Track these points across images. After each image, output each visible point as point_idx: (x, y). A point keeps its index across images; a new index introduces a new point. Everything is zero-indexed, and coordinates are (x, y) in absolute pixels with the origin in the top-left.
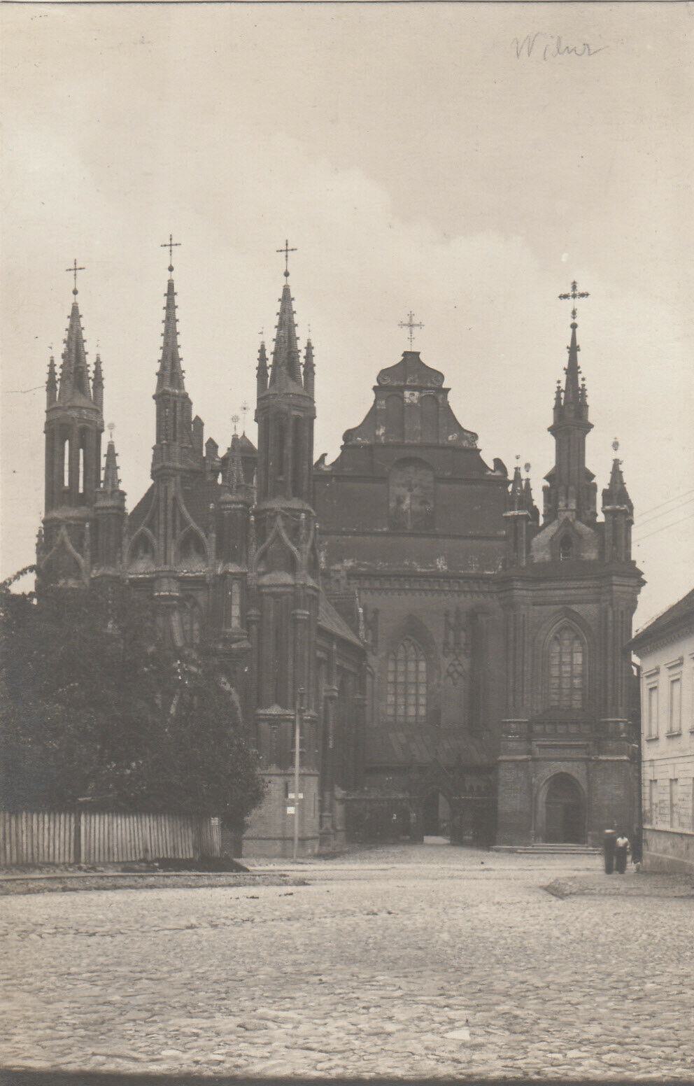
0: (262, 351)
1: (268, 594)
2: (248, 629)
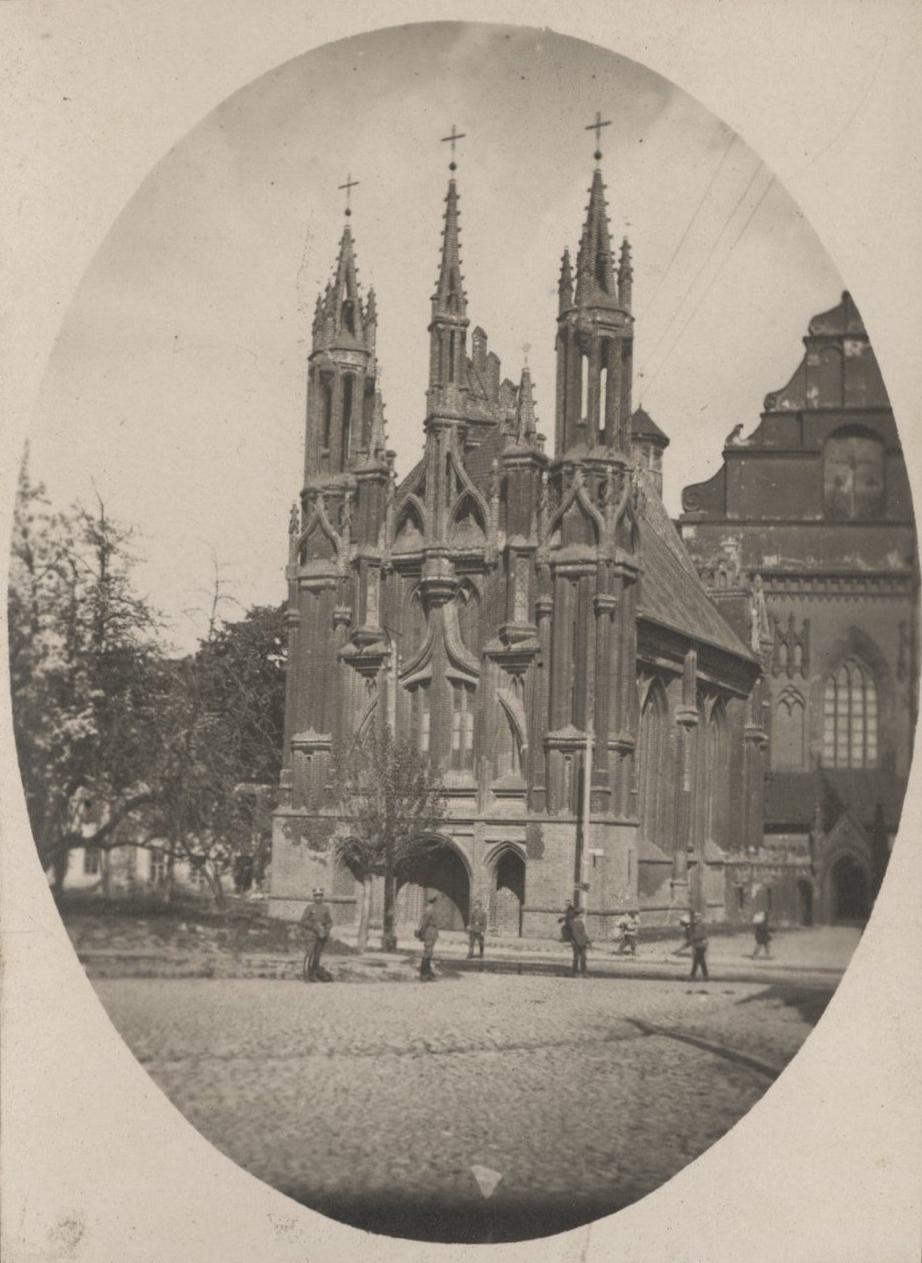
0: (565, 259)
1: (562, 575)
2: (537, 624)
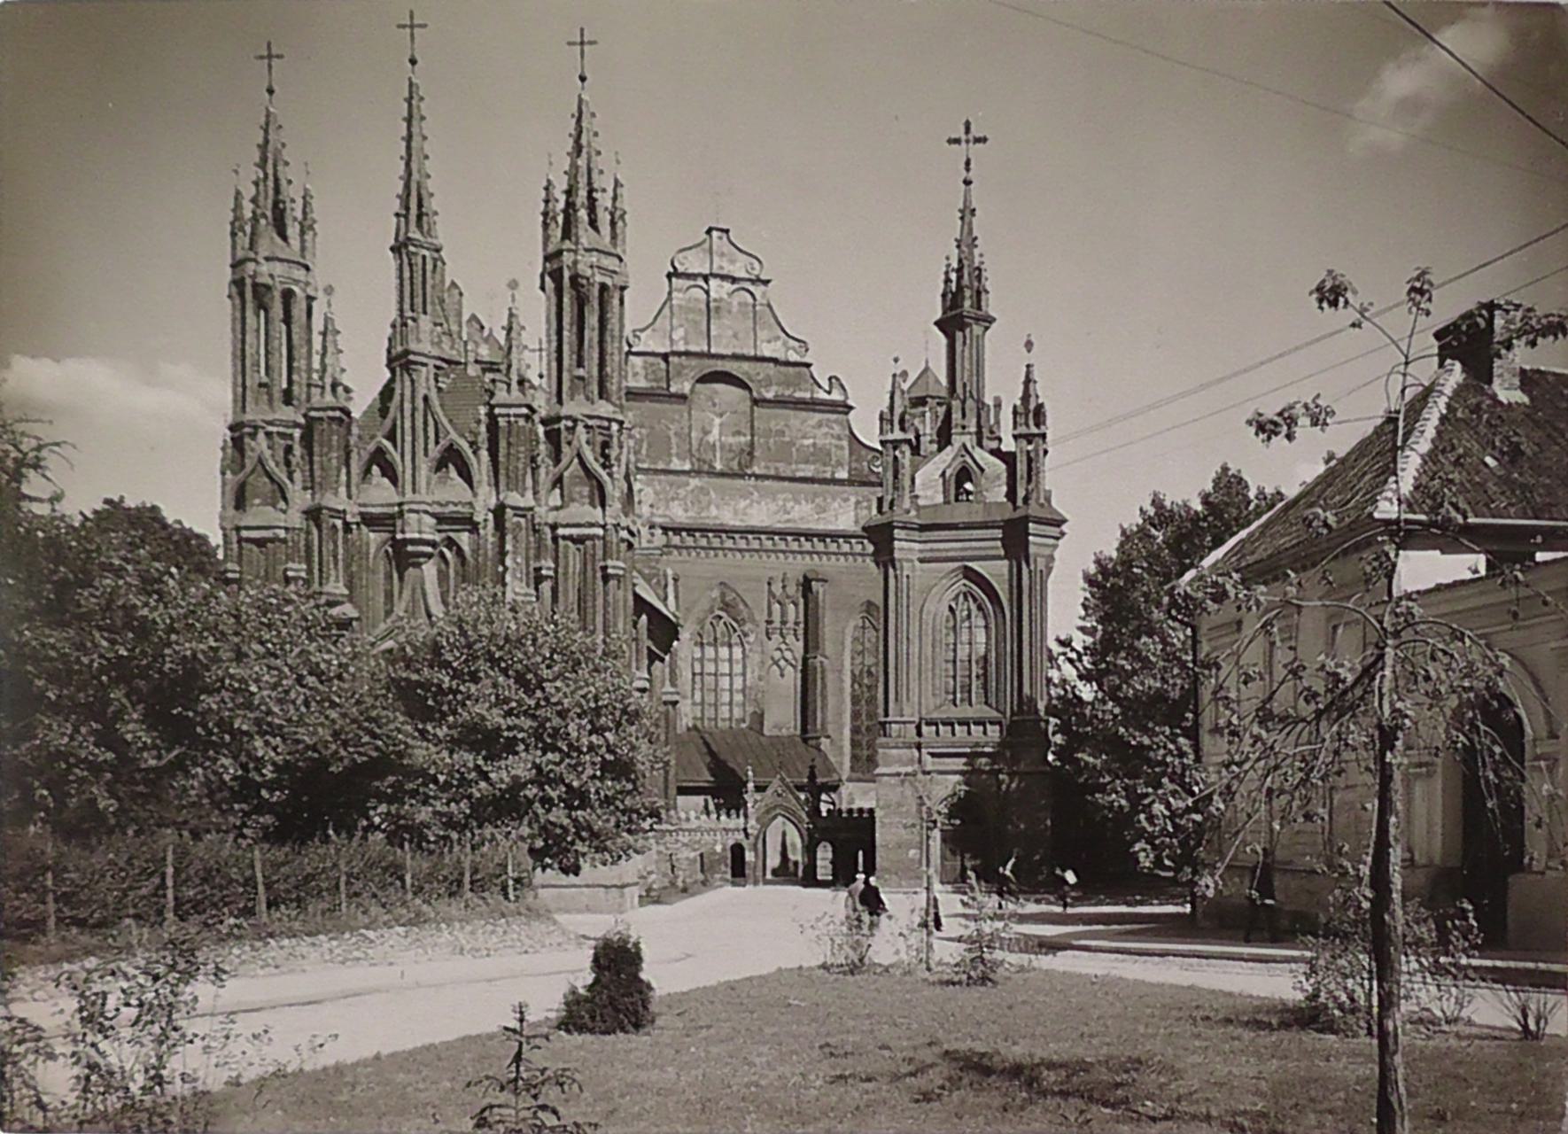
1: (564, 538)
2: (537, 589)
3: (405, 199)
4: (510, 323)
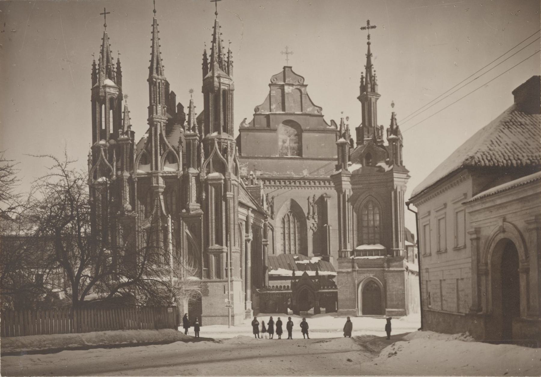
1: (211, 184)
3: (152, 61)
4: (190, 105)
